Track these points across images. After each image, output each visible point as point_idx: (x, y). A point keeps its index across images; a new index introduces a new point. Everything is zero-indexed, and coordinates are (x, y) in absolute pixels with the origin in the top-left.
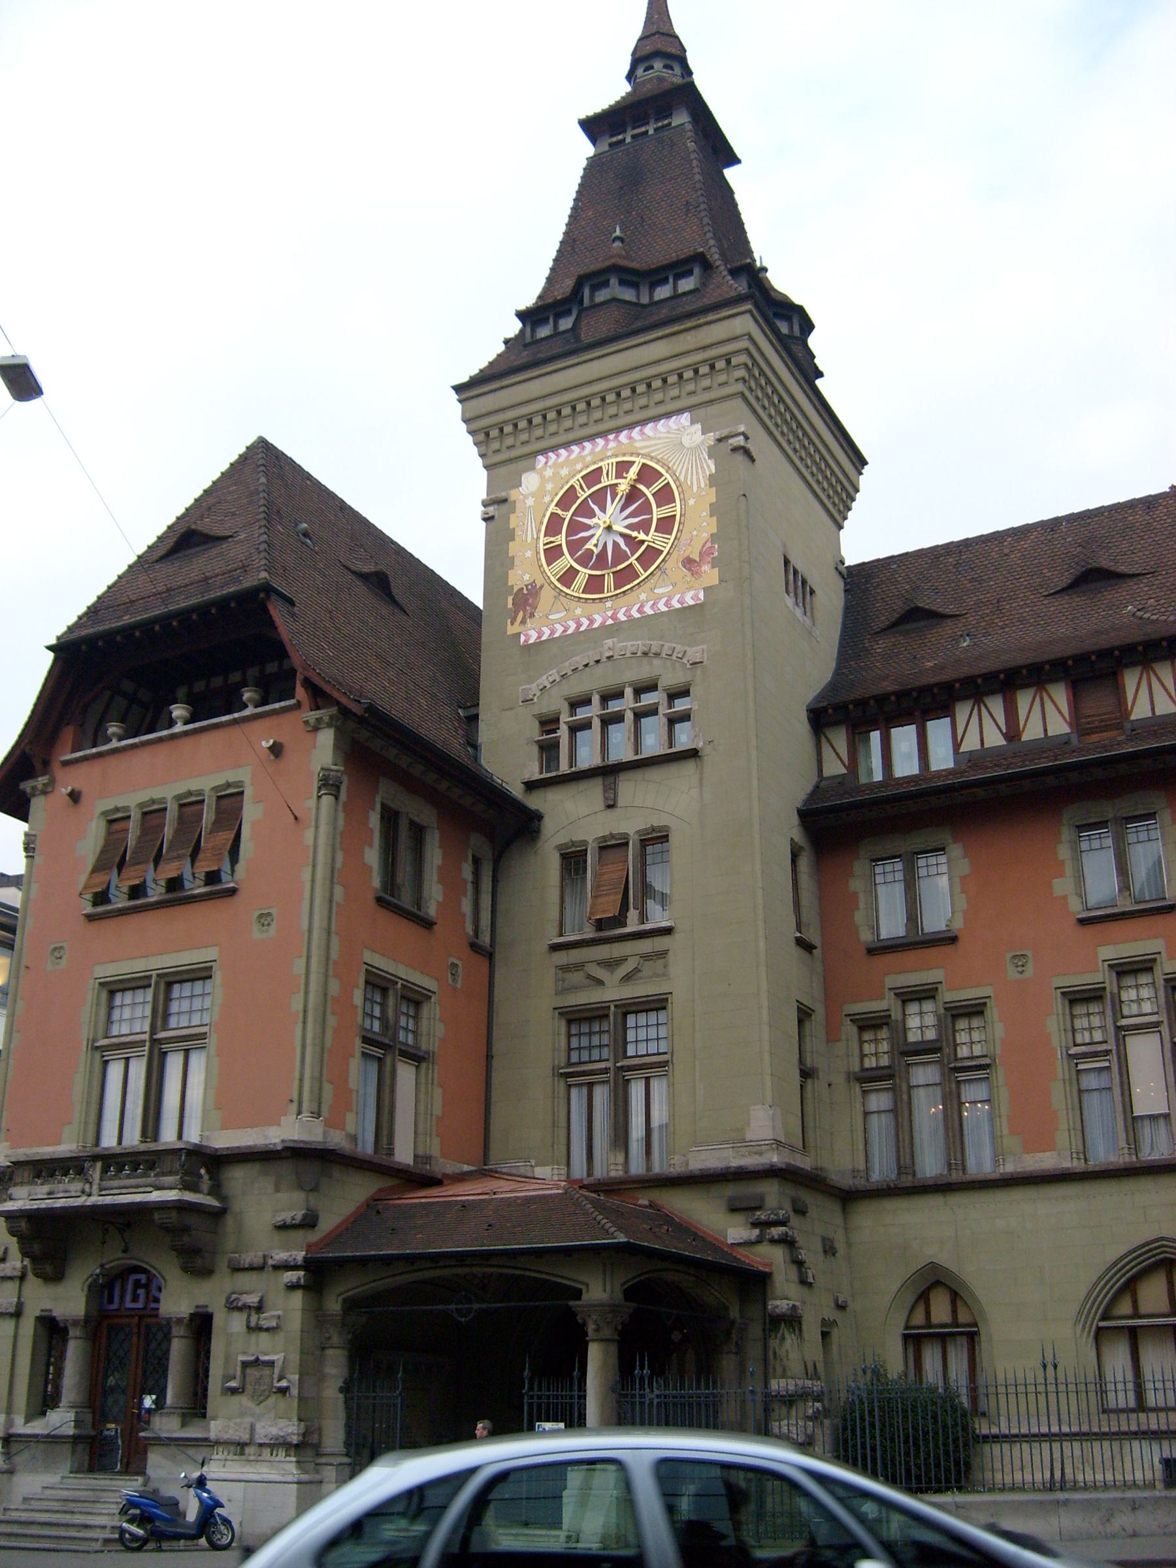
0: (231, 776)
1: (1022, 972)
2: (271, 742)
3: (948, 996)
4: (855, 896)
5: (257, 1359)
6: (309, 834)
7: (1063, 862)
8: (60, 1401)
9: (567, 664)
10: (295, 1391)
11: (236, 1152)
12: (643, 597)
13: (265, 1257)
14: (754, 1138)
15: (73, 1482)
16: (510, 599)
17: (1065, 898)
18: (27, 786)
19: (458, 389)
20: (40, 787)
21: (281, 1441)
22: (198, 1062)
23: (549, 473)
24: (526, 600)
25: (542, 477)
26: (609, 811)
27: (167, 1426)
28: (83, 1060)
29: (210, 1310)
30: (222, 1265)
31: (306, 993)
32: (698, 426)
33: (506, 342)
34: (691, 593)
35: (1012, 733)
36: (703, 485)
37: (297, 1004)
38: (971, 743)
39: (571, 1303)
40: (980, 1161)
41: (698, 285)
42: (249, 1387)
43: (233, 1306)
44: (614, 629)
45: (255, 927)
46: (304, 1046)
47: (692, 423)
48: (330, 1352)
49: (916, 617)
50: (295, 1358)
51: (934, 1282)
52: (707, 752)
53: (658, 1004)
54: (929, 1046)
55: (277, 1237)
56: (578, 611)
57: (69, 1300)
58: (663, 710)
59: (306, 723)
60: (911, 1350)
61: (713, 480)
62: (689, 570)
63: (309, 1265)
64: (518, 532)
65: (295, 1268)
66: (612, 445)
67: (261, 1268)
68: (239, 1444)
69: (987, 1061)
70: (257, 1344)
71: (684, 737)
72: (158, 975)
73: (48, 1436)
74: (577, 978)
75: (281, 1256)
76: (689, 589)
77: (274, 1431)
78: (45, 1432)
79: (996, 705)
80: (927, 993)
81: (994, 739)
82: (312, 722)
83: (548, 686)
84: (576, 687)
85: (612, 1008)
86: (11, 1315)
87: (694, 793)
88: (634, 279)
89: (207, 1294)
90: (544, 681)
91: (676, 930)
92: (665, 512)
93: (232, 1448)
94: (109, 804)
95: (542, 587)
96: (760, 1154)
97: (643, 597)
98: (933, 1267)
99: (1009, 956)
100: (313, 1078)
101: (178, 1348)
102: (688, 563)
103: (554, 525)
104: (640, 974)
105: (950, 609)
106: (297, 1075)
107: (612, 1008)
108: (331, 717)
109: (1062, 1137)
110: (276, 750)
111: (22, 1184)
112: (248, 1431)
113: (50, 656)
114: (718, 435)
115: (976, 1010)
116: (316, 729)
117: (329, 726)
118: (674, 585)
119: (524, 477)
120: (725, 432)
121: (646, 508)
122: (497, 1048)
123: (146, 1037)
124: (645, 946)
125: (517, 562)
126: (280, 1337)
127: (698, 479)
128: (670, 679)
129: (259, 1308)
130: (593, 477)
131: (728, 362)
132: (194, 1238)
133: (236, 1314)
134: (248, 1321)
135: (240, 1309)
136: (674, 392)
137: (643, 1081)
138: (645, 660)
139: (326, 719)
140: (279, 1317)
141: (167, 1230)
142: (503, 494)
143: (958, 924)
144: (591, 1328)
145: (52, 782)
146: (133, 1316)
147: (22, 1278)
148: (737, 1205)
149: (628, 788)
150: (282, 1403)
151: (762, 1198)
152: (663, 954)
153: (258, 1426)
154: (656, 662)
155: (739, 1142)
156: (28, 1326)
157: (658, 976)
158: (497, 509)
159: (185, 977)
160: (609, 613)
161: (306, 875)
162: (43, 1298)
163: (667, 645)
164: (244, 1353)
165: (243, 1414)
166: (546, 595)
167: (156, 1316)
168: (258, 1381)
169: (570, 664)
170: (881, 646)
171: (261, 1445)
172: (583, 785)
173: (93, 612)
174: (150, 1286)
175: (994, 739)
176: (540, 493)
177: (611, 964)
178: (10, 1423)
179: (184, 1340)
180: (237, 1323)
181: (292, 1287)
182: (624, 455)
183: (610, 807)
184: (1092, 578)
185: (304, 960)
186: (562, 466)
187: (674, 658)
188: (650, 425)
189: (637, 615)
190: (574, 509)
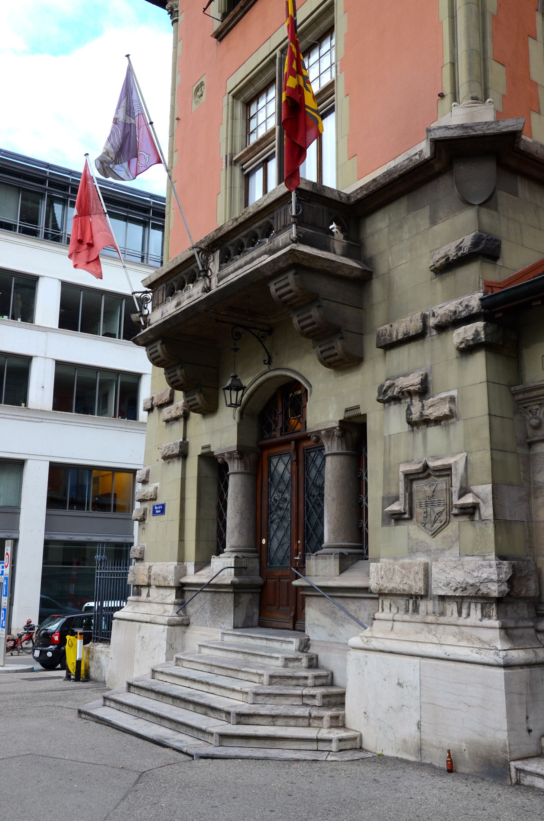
5: (426, 467)
8: (224, 547)
10: (487, 511)
13: (425, 318)
29: (362, 411)
30: (372, 350)
42: (418, 511)
43: (389, 397)
46: (453, 17)
50: (483, 458)
68: (410, 596)
73: (209, 585)
75: (444, 308)
77: (459, 577)
93: (402, 602)
100: (470, 51)
106: (447, 59)
112: (421, 576)
126: (458, 429)
129: (423, 391)
134: (409, 412)
135: (396, 400)
140: (452, 399)
147: (186, 417)
153: (434, 571)
164: (408, 462)
165: (412, 551)
168: (431, 501)
171: (443, 598)
178: (181, 571)
181: (467, 350)
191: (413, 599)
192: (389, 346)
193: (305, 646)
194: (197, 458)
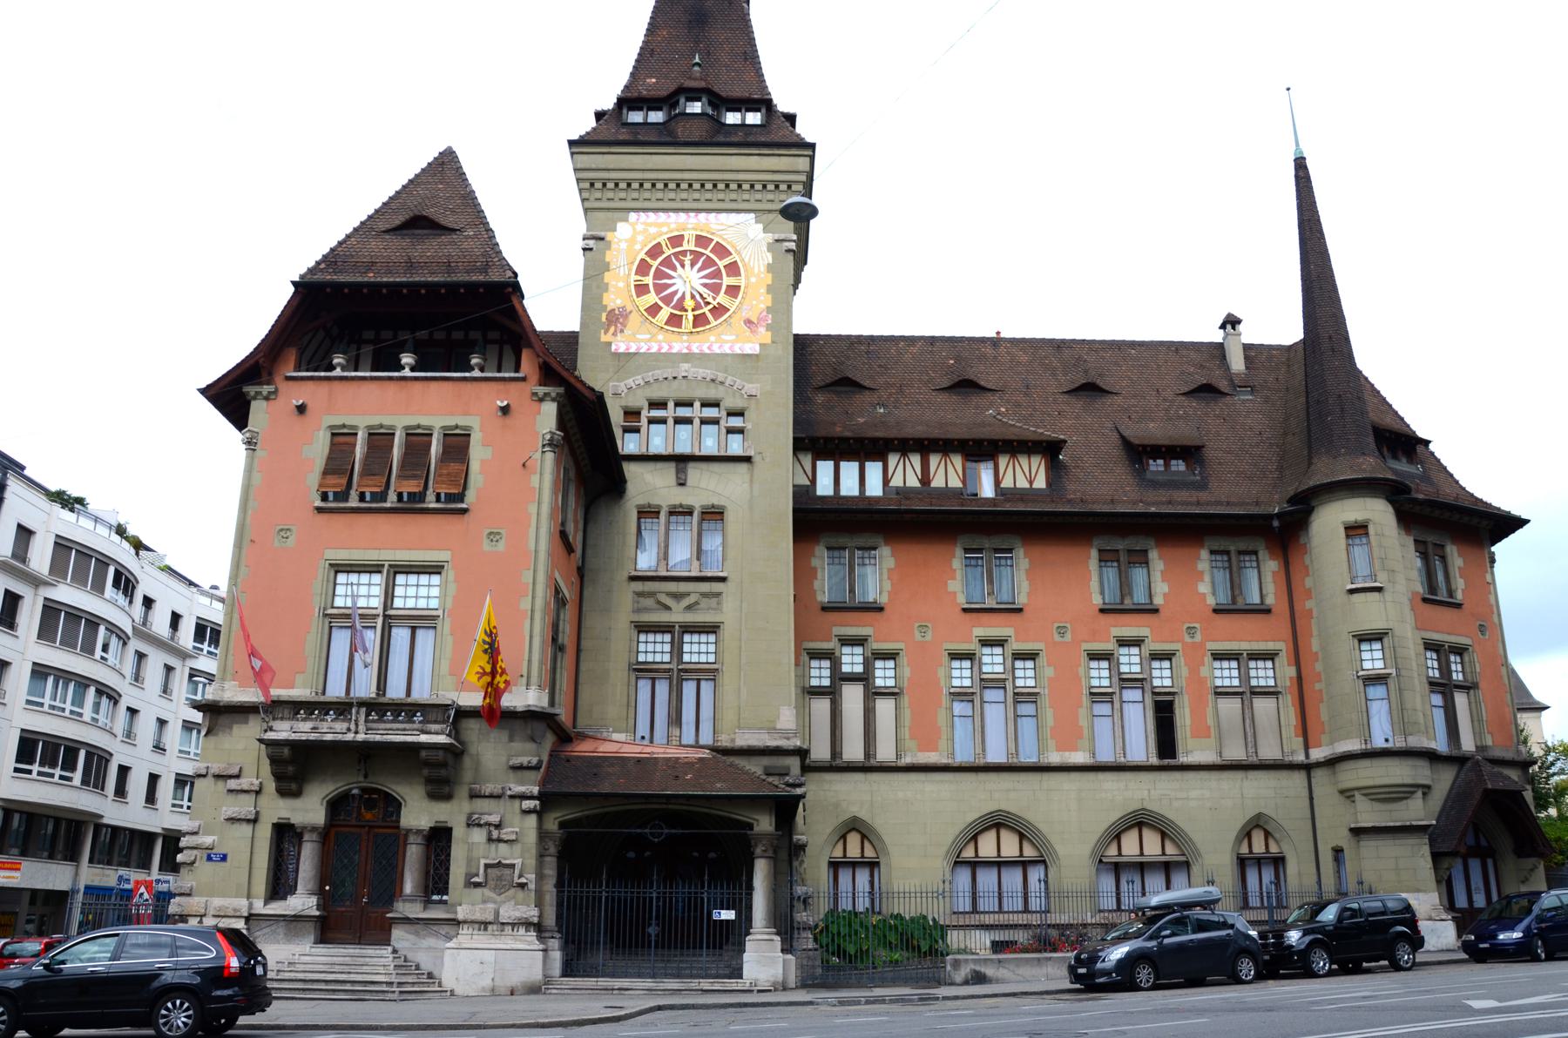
3: (875, 646)
4: (815, 570)
10: (532, 886)
12: (712, 338)
15: (322, 949)
17: (955, 593)
18: (251, 390)
19: (571, 143)
23: (640, 227)
24: (617, 319)
27: (414, 910)
28: (316, 626)
30: (463, 792)
31: (533, 598)
32: (761, 226)
33: (599, 115)
35: (925, 479)
37: (526, 604)
38: (897, 481)
40: (885, 752)
42: (492, 883)
44: (688, 357)
45: (486, 542)
48: (548, 859)
49: (847, 384)
50: (532, 862)
51: (855, 826)
52: (756, 459)
53: (712, 629)
55: (511, 774)
57: (310, 810)
58: (723, 423)
59: (535, 394)
61: (770, 268)
63: (541, 797)
64: (612, 266)
65: (531, 798)
67: (499, 797)
71: (735, 446)
74: (649, 602)
77: (518, 914)
79: (916, 459)
80: (859, 641)
81: (913, 482)
82: (541, 394)
84: (657, 393)
86: (248, 821)
87: (746, 486)
89: (451, 813)
90: (630, 382)
92: (732, 281)
98: (855, 819)
101: (413, 853)
102: (748, 322)
103: (643, 268)
105: (867, 383)
109: (943, 744)
110: (505, 410)
113: (292, 289)
116: (541, 400)
119: (620, 225)
120: (782, 236)
121: (717, 274)
123: (380, 611)
124: (705, 587)
125: (611, 289)
126: (517, 848)
128: (730, 402)
129: (498, 826)
130: (676, 240)
131: (789, 187)
133: (476, 830)
135: (479, 825)
136: (746, 196)
141: (427, 764)
142: (602, 234)
143: (883, 600)
144: (758, 851)
145: (276, 392)
149: (694, 472)
150: (520, 894)
152: (718, 595)
154: (721, 388)
155: (772, 730)
156: (265, 832)
158: (594, 244)
161: (533, 509)
162: (277, 809)
165: (484, 902)
166: (634, 319)
167: (398, 827)
168: (500, 878)
170: (820, 398)
172: (660, 465)
173: (332, 259)
174: (393, 805)
175: (913, 482)
176: (632, 241)
177: (678, 596)
180: (478, 836)
184: (966, 386)
186: (650, 225)
190: (657, 263)
191: (484, 925)
192: (474, 796)
193: (395, 951)
194: (269, 827)
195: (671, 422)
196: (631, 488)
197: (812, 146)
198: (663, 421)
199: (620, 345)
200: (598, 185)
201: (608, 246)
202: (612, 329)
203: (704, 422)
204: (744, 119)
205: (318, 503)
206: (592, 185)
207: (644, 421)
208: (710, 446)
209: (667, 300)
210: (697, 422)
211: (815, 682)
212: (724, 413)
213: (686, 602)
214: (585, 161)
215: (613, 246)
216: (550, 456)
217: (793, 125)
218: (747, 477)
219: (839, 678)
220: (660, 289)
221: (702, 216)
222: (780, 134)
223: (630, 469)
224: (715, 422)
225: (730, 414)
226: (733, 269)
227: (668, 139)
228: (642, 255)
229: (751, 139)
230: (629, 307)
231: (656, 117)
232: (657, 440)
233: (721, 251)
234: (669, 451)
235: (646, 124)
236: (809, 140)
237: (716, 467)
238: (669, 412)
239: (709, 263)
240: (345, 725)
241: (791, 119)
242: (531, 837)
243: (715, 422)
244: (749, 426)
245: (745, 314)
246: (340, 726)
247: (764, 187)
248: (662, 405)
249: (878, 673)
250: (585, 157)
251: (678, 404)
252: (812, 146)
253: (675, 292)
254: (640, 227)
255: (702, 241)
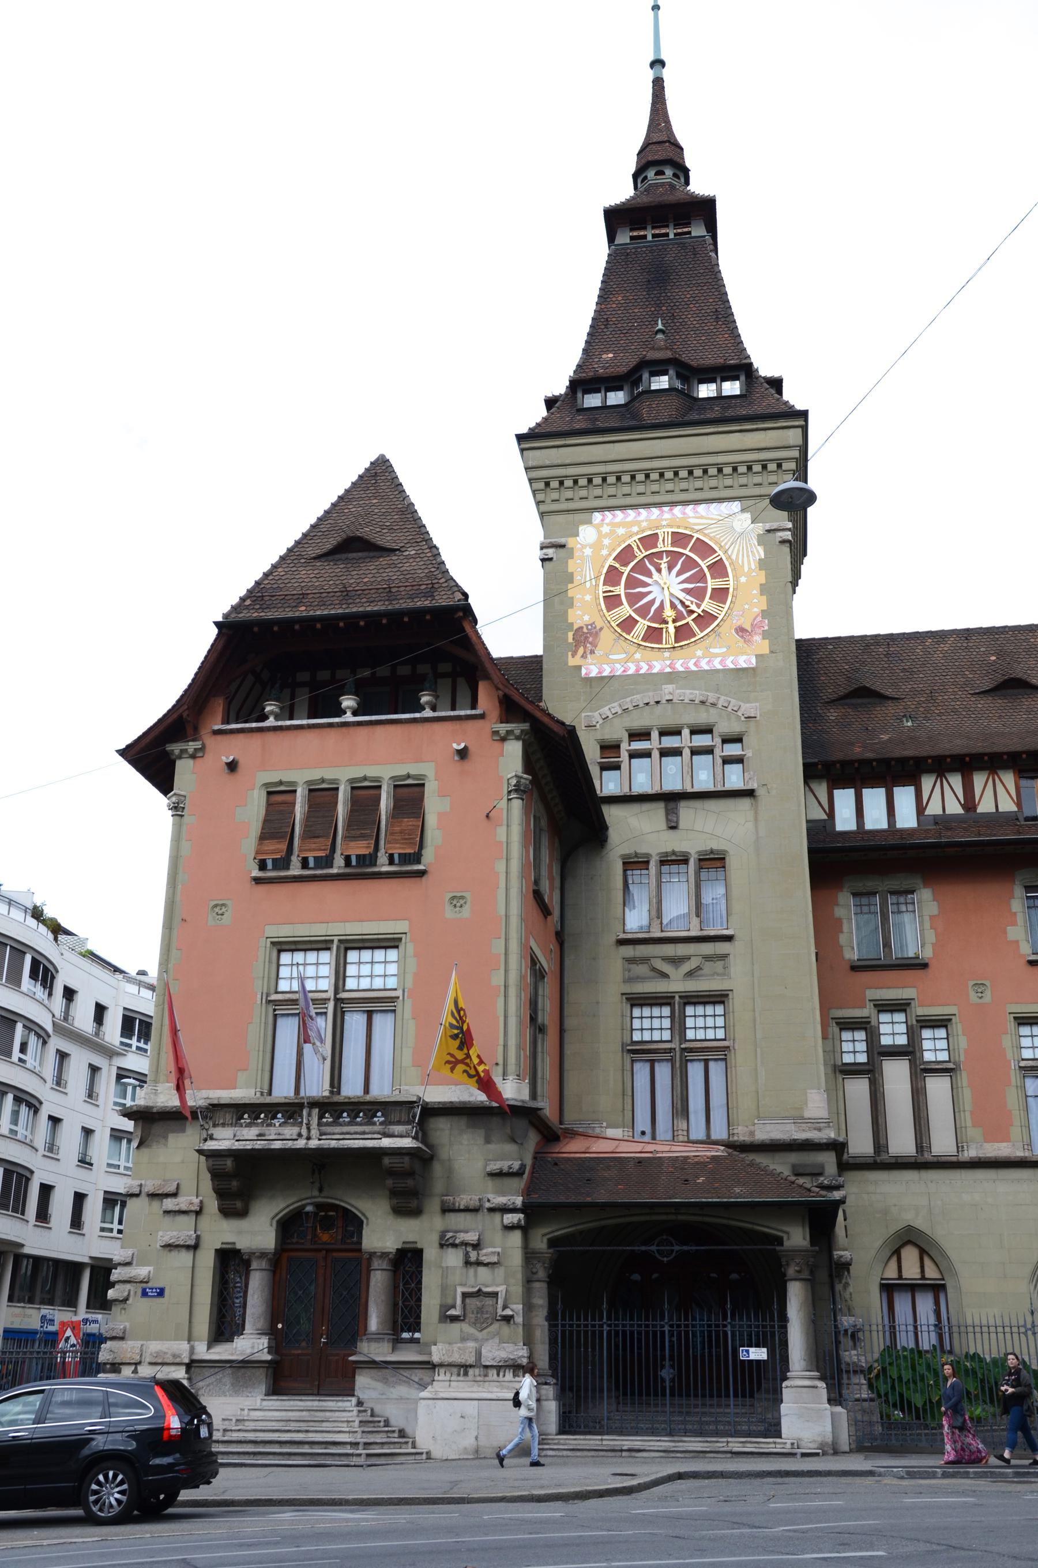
0: (413, 769)
1: (981, 998)
2: (462, 746)
3: (921, 1011)
4: (839, 921)
5: (480, 1290)
6: (501, 833)
7: (1015, 914)
8: (244, 1329)
9: (628, 699)
10: (519, 1319)
11: (448, 1105)
12: (699, 653)
13: (480, 1200)
14: (809, 1116)
15: (275, 1402)
16: (570, 635)
17: (1017, 942)
18: (175, 748)
19: (520, 438)
20: (191, 751)
21: (510, 1363)
22: (383, 1024)
23: (605, 529)
24: (585, 638)
25: (599, 532)
26: (671, 831)
27: (379, 1351)
28: (259, 1015)
29: (419, 1246)
31: (506, 971)
32: (747, 516)
34: (744, 657)
35: (969, 803)
36: (753, 567)
37: (497, 979)
38: (934, 808)
39: (778, 1248)
40: (942, 1144)
41: (744, 392)
42: (471, 1316)
43: (445, 1244)
44: (672, 677)
45: (448, 908)
46: (506, 1017)
47: (743, 510)
48: (537, 1285)
49: (864, 695)
50: (518, 1289)
51: (909, 1238)
53: (719, 998)
54: (901, 1050)
55: (490, 1183)
56: (638, 656)
57: (257, 1232)
58: (718, 752)
59: (496, 733)
60: (885, 1296)
61: (762, 564)
62: (742, 637)
64: (577, 578)
66: (667, 516)
67: (475, 1210)
68: (462, 1366)
69: (951, 1066)
70: (476, 1275)
71: (735, 778)
72: (339, 941)
73: (242, 1361)
74: (642, 969)
75: (500, 1200)
76: (743, 654)
77: (503, 1355)
78: (241, 1358)
79: (956, 781)
80: (900, 1006)
81: (954, 808)
82: (503, 733)
83: (611, 716)
84: (639, 722)
85: (677, 998)
86: (188, 1247)
87: (750, 825)
88: (687, 373)
89: (421, 1231)
90: (605, 711)
91: (736, 938)
93: (455, 1370)
94: (273, 777)
95: (601, 629)
96: (820, 1130)
97: (699, 653)
98: (910, 1229)
99: (971, 983)
101: (379, 1281)
102: (741, 630)
103: (612, 576)
104: (700, 972)
105: (889, 692)
106: (501, 1042)
107: (677, 998)
108: (522, 731)
109: (1016, 1132)
110: (463, 754)
111: (223, 1125)
113: (215, 631)
114: (768, 526)
115: (941, 1023)
116: (503, 739)
117: (517, 738)
118: (729, 647)
119: (582, 529)
121: (701, 577)
122: (570, 1022)
123: (331, 994)
124: (707, 948)
126: (500, 1272)
127: (749, 561)
128: (724, 727)
129: (477, 1246)
130: (649, 541)
131: (779, 466)
132: (408, 1181)
133: (451, 1251)
135: (454, 1245)
137: (702, 1064)
138: (703, 707)
139: (517, 732)
141: (391, 1173)
142: (562, 541)
143: (927, 954)
144: (791, 1271)
145: (203, 749)
146: (319, 1250)
148: (801, 1171)
149: (686, 812)
150: (506, 1329)
151: (822, 1166)
152: (724, 957)
153: (484, 1351)
154: (712, 711)
155: (799, 1119)
156: (207, 1260)
157: (718, 975)
158: (554, 554)
159: (367, 945)
160: (668, 662)
161: (500, 867)
162: (221, 1232)
163: (723, 698)
164: (464, 1285)
165: (464, 1339)
166: (606, 638)
167: (360, 1250)
168: (480, 1310)
169: (631, 701)
170: (833, 714)
171: (486, 1367)
172: (646, 806)
173: (257, 594)
174: (354, 1224)
175: (954, 808)
176: (597, 546)
177: (676, 961)
179: (385, 1273)
180: (454, 1258)
182: (679, 527)
183: (673, 828)
184: (1013, 686)
185: (503, 941)
186: (619, 525)
187: (729, 709)
188: (703, 506)
189: (694, 668)
190: (630, 567)
191: (464, 1368)
192: (447, 1209)
193: (360, 1403)
194: (212, 1254)
195: (656, 754)
196: (614, 835)
197: (804, 414)
198: (646, 754)
199: (591, 669)
200: (554, 484)
201: (571, 554)
202: (581, 650)
203: (695, 752)
204: (719, 389)
205: (256, 873)
206: (547, 484)
207: (624, 756)
208: (704, 779)
209: (643, 612)
210: (686, 752)
211: (848, 1059)
212: (718, 741)
213: (686, 967)
214: (539, 457)
215: (577, 554)
216: (517, 805)
217: (780, 392)
218: (750, 815)
219: (878, 1053)
220: (633, 599)
221: (678, 510)
222: (765, 404)
223: (612, 814)
224: (709, 751)
225: (725, 741)
226: (718, 569)
227: (634, 423)
228: (610, 561)
229: (730, 413)
230: (599, 624)
231: (617, 398)
232: (642, 777)
233: (704, 548)
234: (656, 789)
235: (605, 407)
236: (799, 406)
237: (712, 805)
238: (654, 743)
239: (690, 564)
240: (295, 1130)
241: (776, 384)
242: (516, 1258)
243: (709, 751)
244: (749, 753)
245: (736, 622)
246: (290, 1131)
247: (750, 468)
248: (643, 735)
249: (927, 1045)
250: (537, 453)
251: (663, 733)
252: (804, 414)
253: (653, 601)
254: (605, 529)
255: (679, 539)
